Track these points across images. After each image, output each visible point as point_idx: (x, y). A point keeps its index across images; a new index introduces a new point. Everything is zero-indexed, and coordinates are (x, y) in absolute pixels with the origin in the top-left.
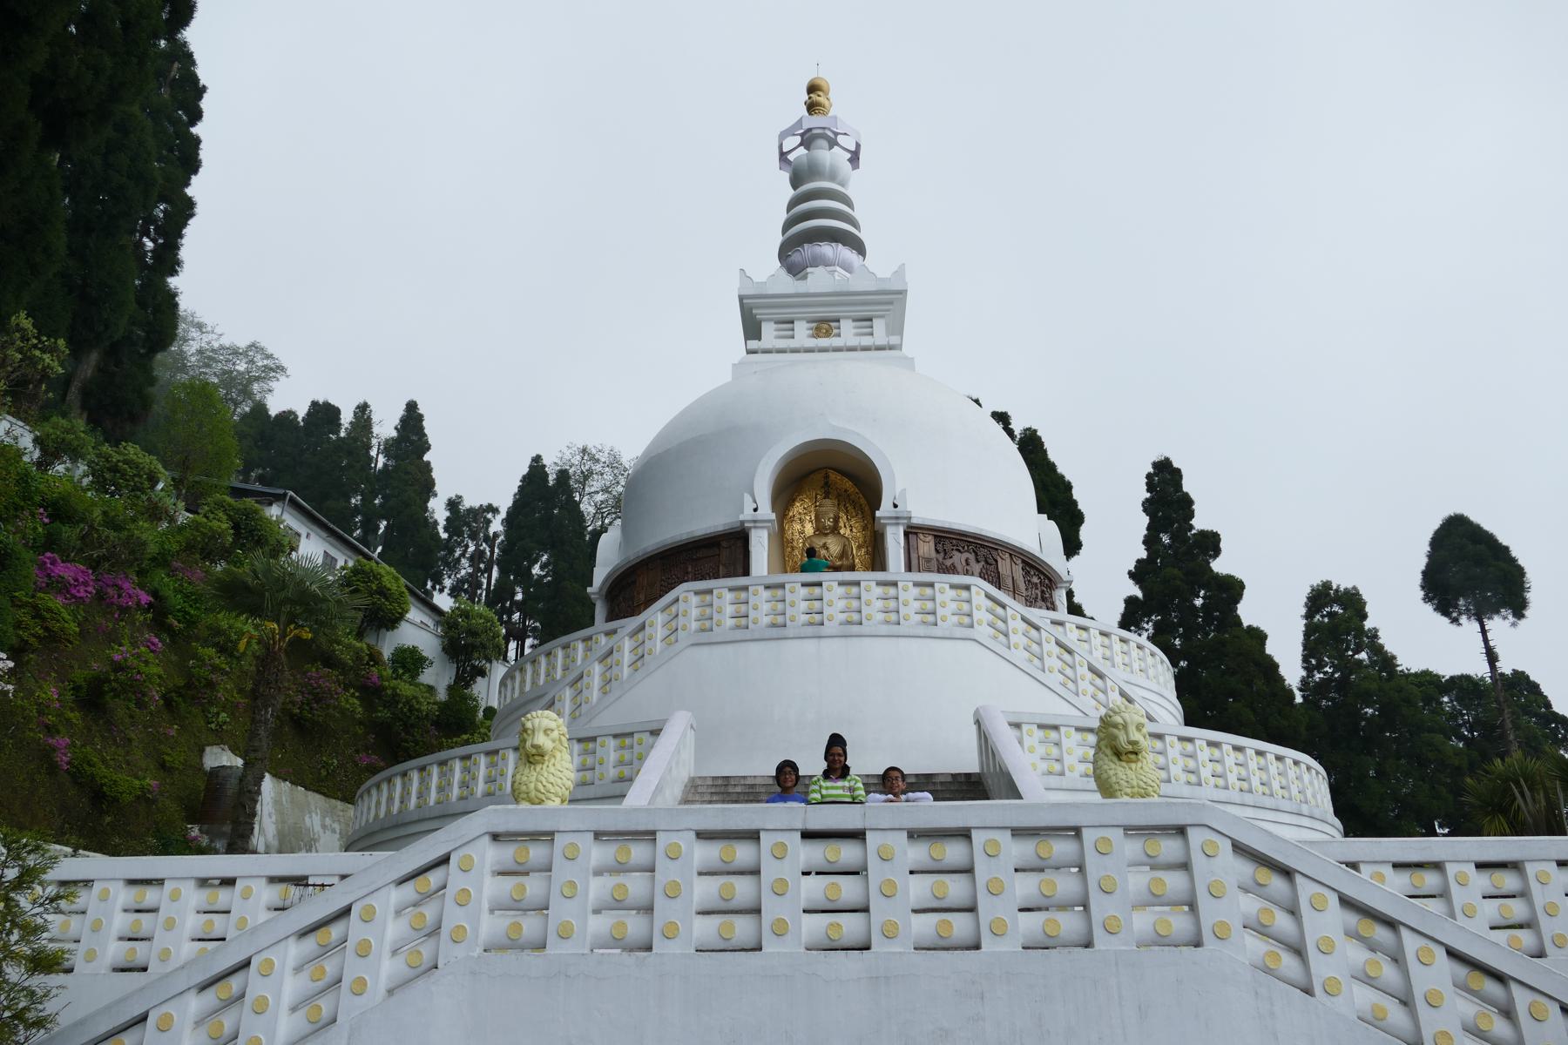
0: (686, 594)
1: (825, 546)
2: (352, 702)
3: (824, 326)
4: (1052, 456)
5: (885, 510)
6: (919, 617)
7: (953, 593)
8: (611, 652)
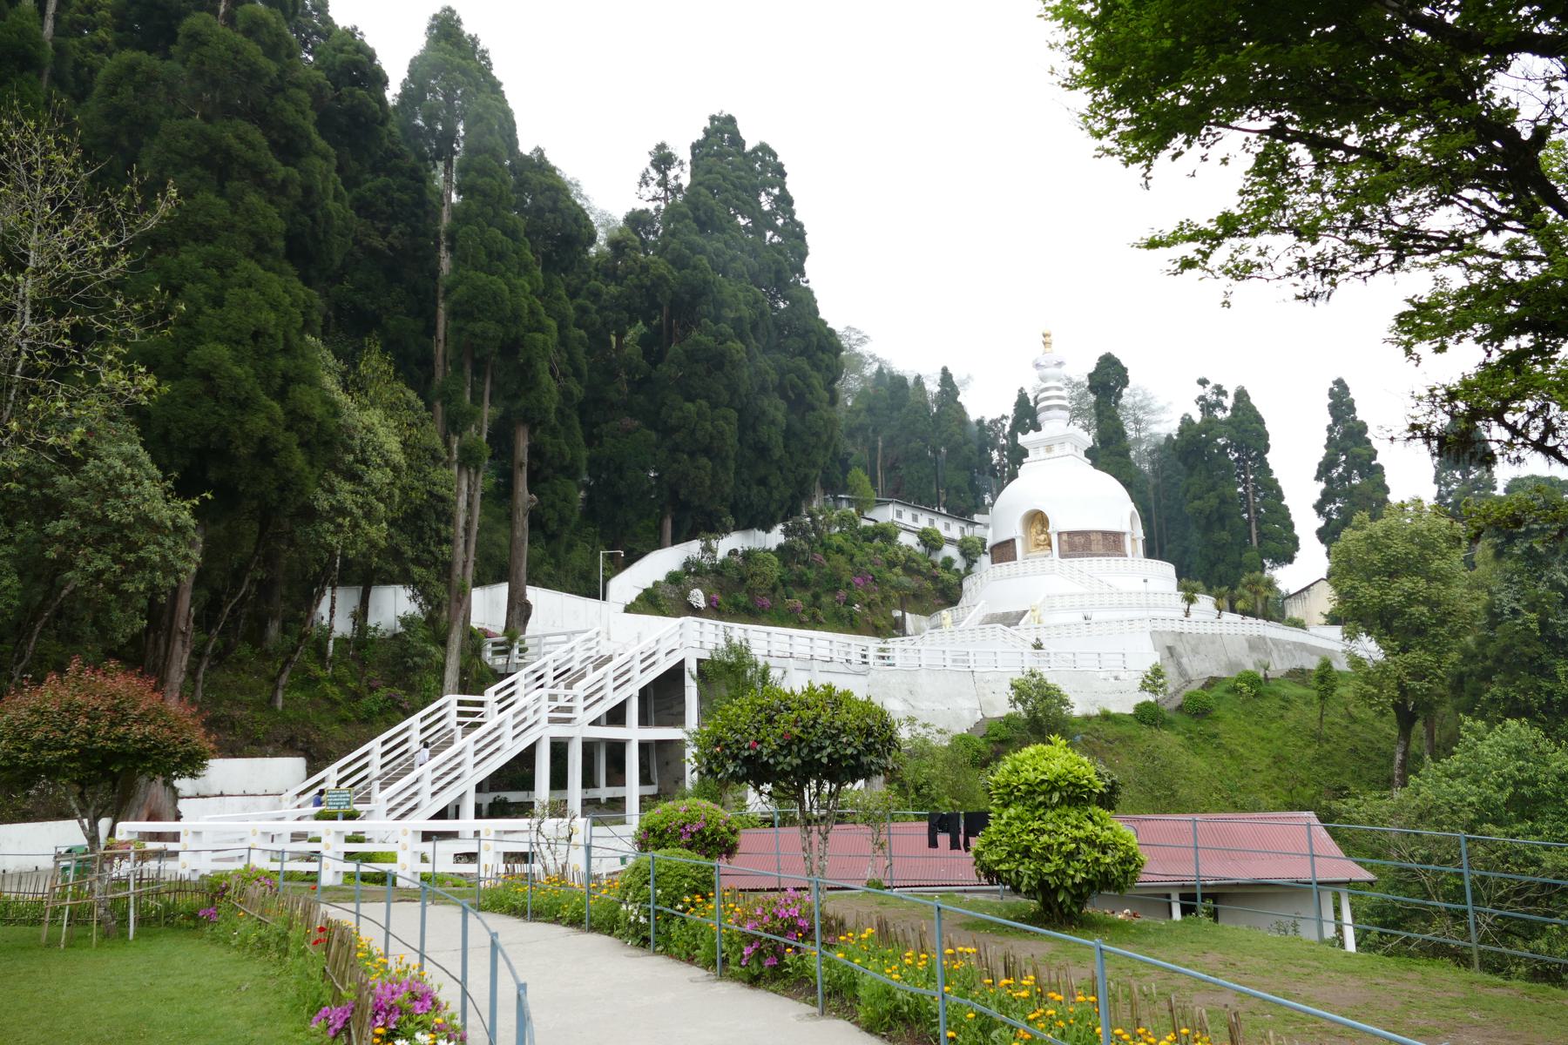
2: (929, 584)
3: (1049, 448)
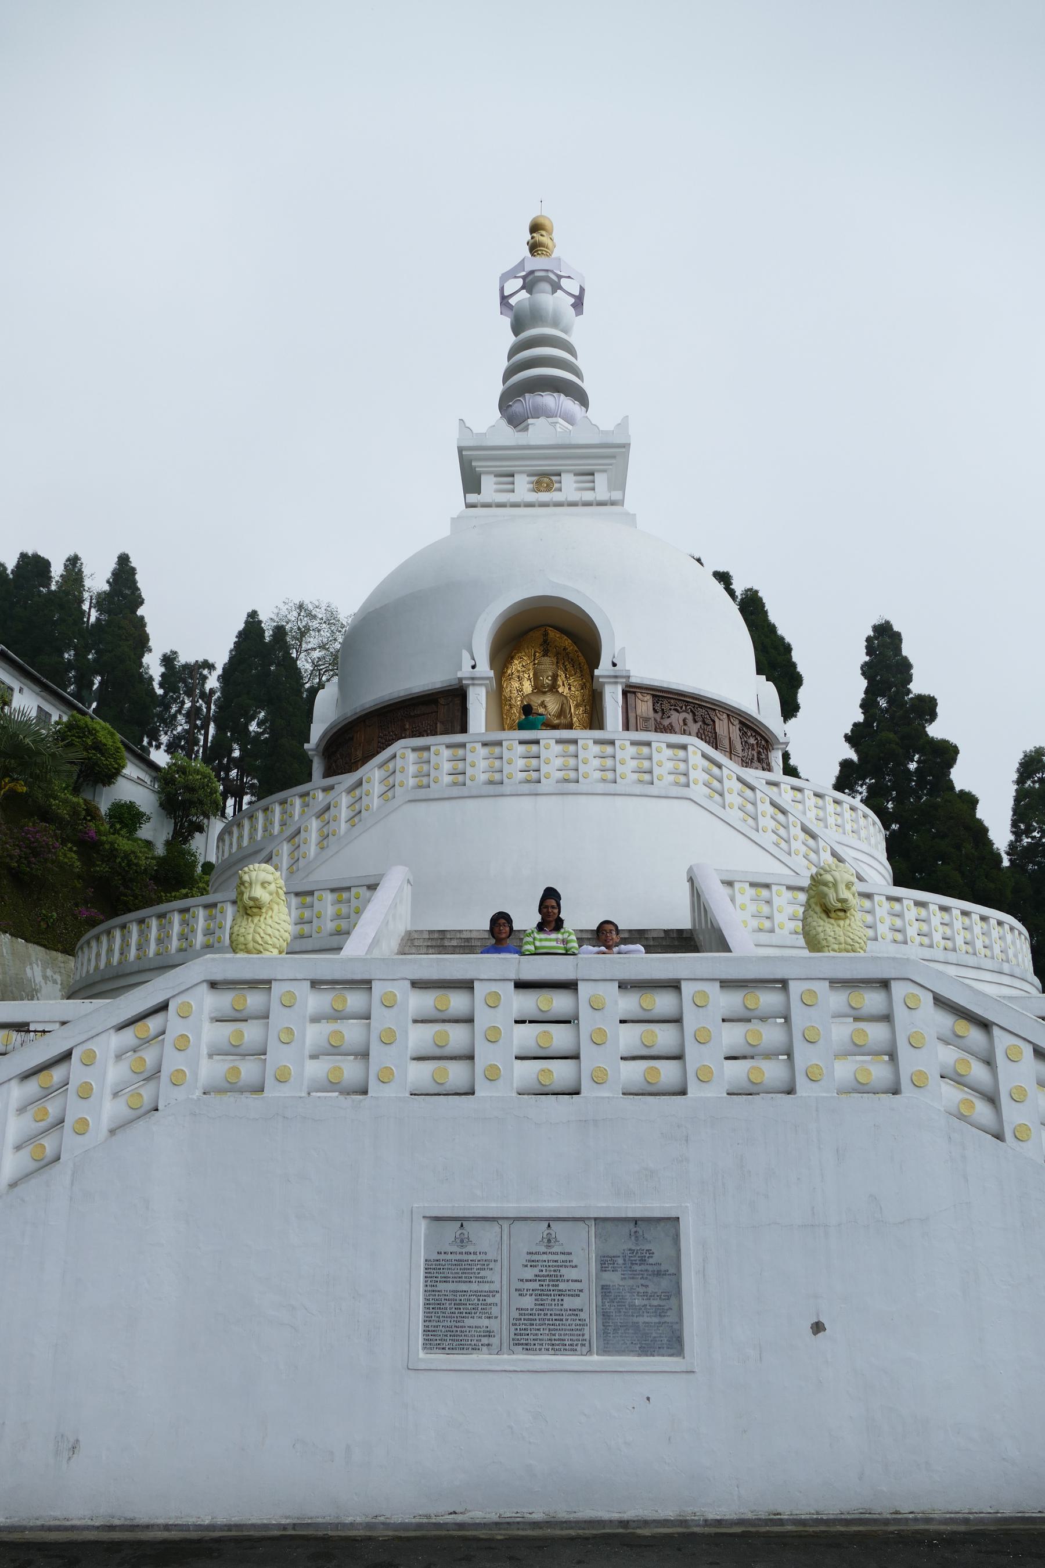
0: (404, 752)
1: (543, 704)
2: (70, 856)
3: (545, 480)
4: (773, 618)
5: (603, 669)
6: (635, 776)
7: (670, 752)
8: (328, 808)
